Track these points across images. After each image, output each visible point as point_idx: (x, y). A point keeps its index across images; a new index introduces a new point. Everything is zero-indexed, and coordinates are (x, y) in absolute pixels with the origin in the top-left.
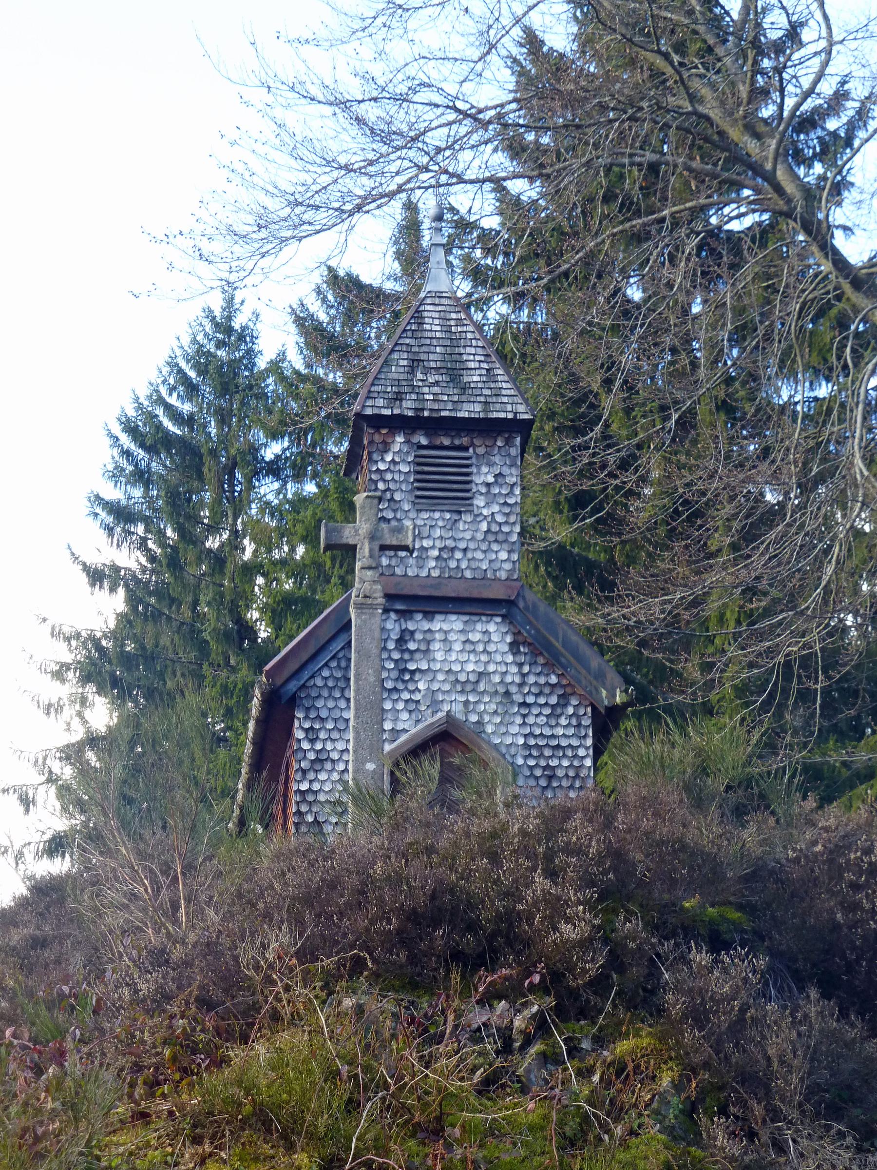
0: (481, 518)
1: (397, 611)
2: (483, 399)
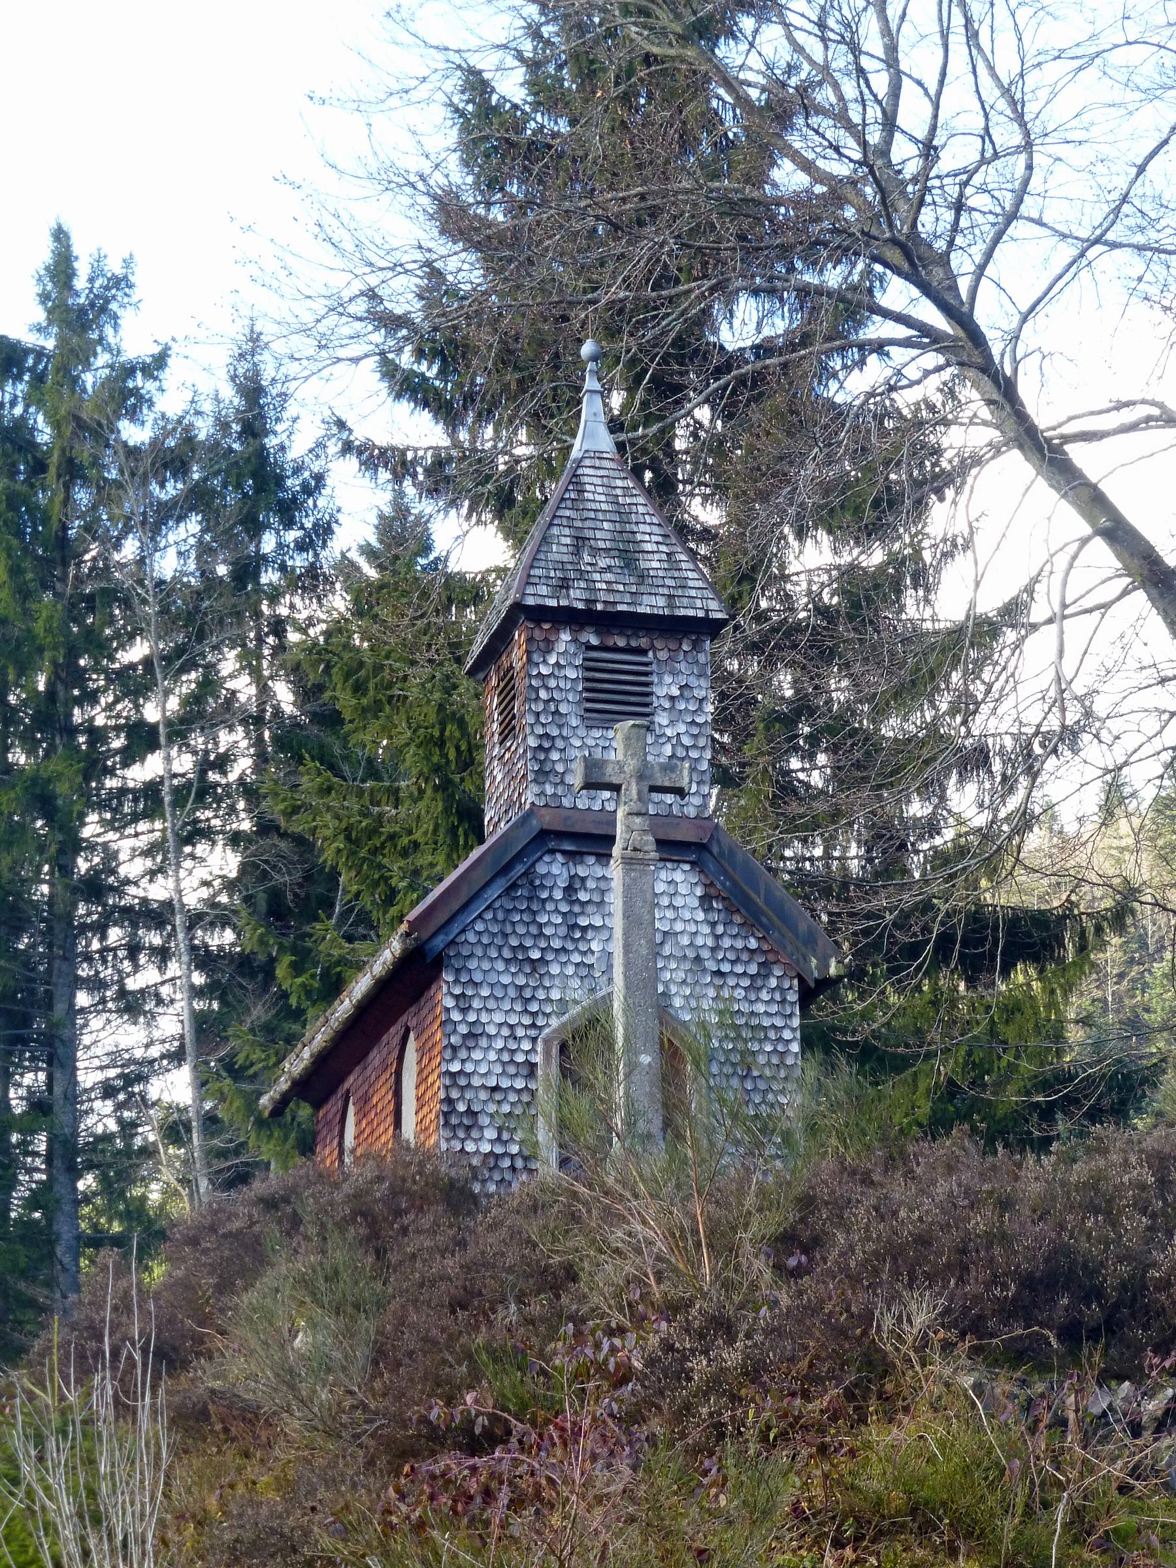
1: (564, 852)
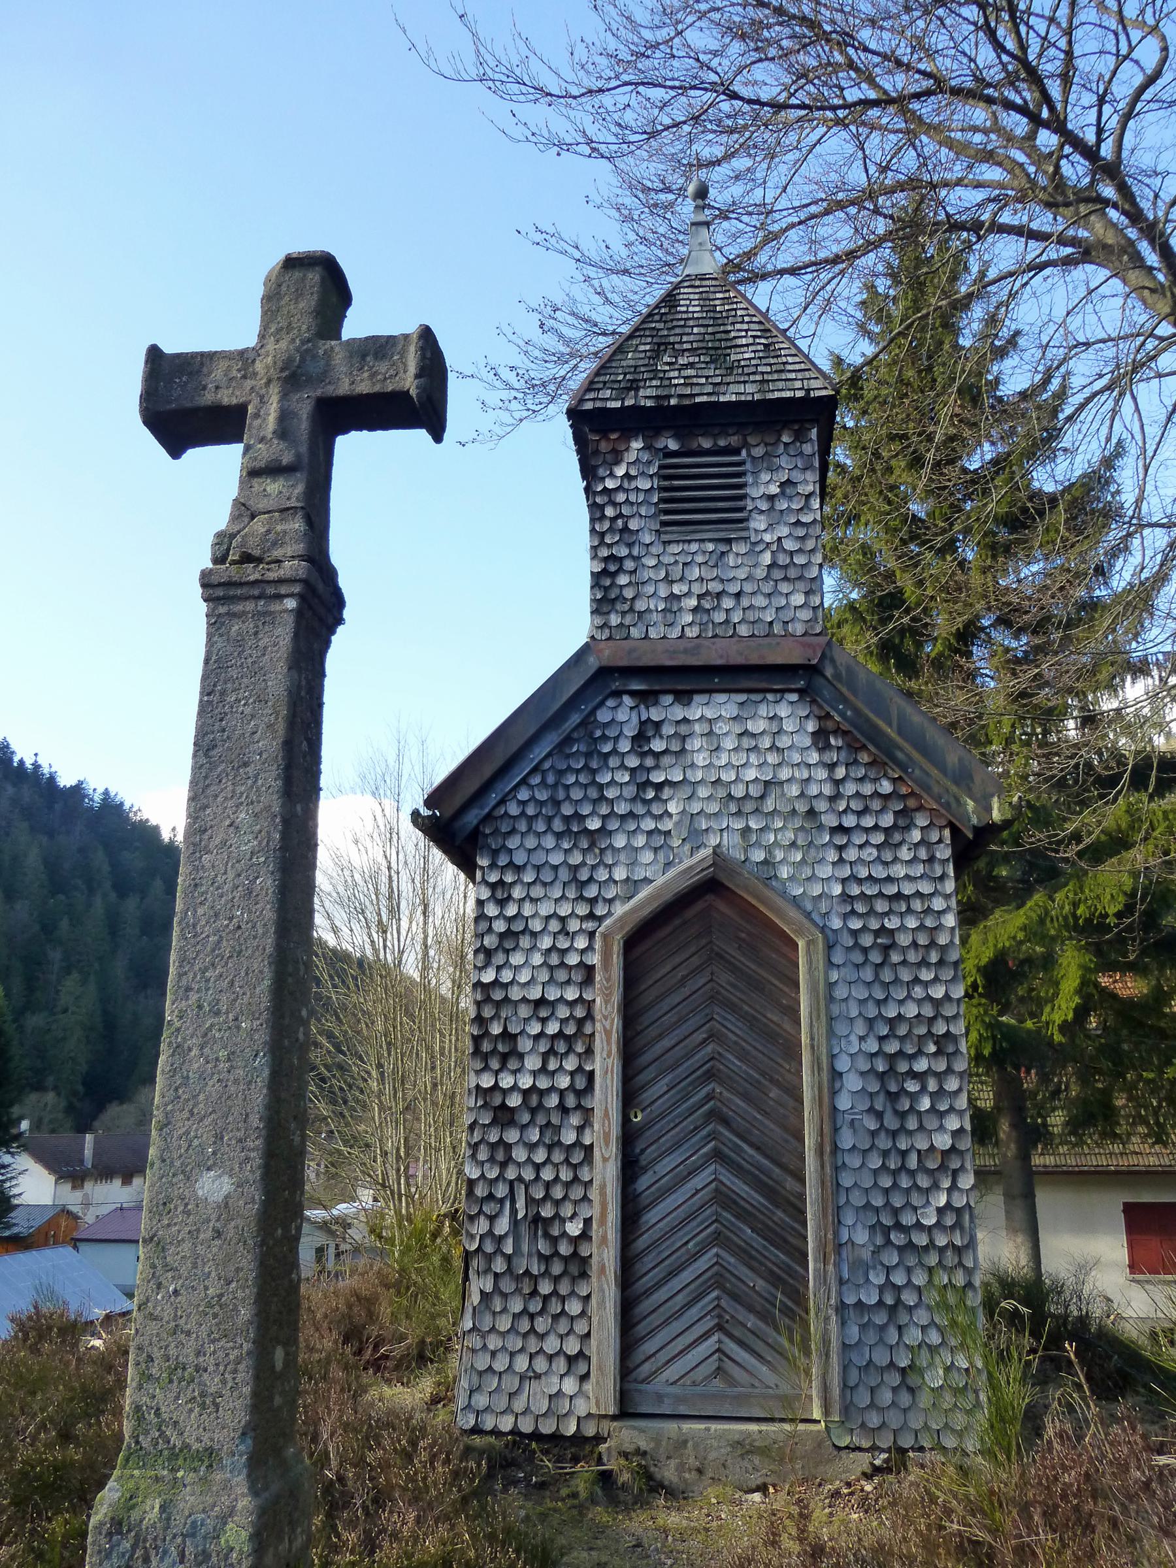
0: (762, 547)
1: (632, 693)
2: (758, 378)
